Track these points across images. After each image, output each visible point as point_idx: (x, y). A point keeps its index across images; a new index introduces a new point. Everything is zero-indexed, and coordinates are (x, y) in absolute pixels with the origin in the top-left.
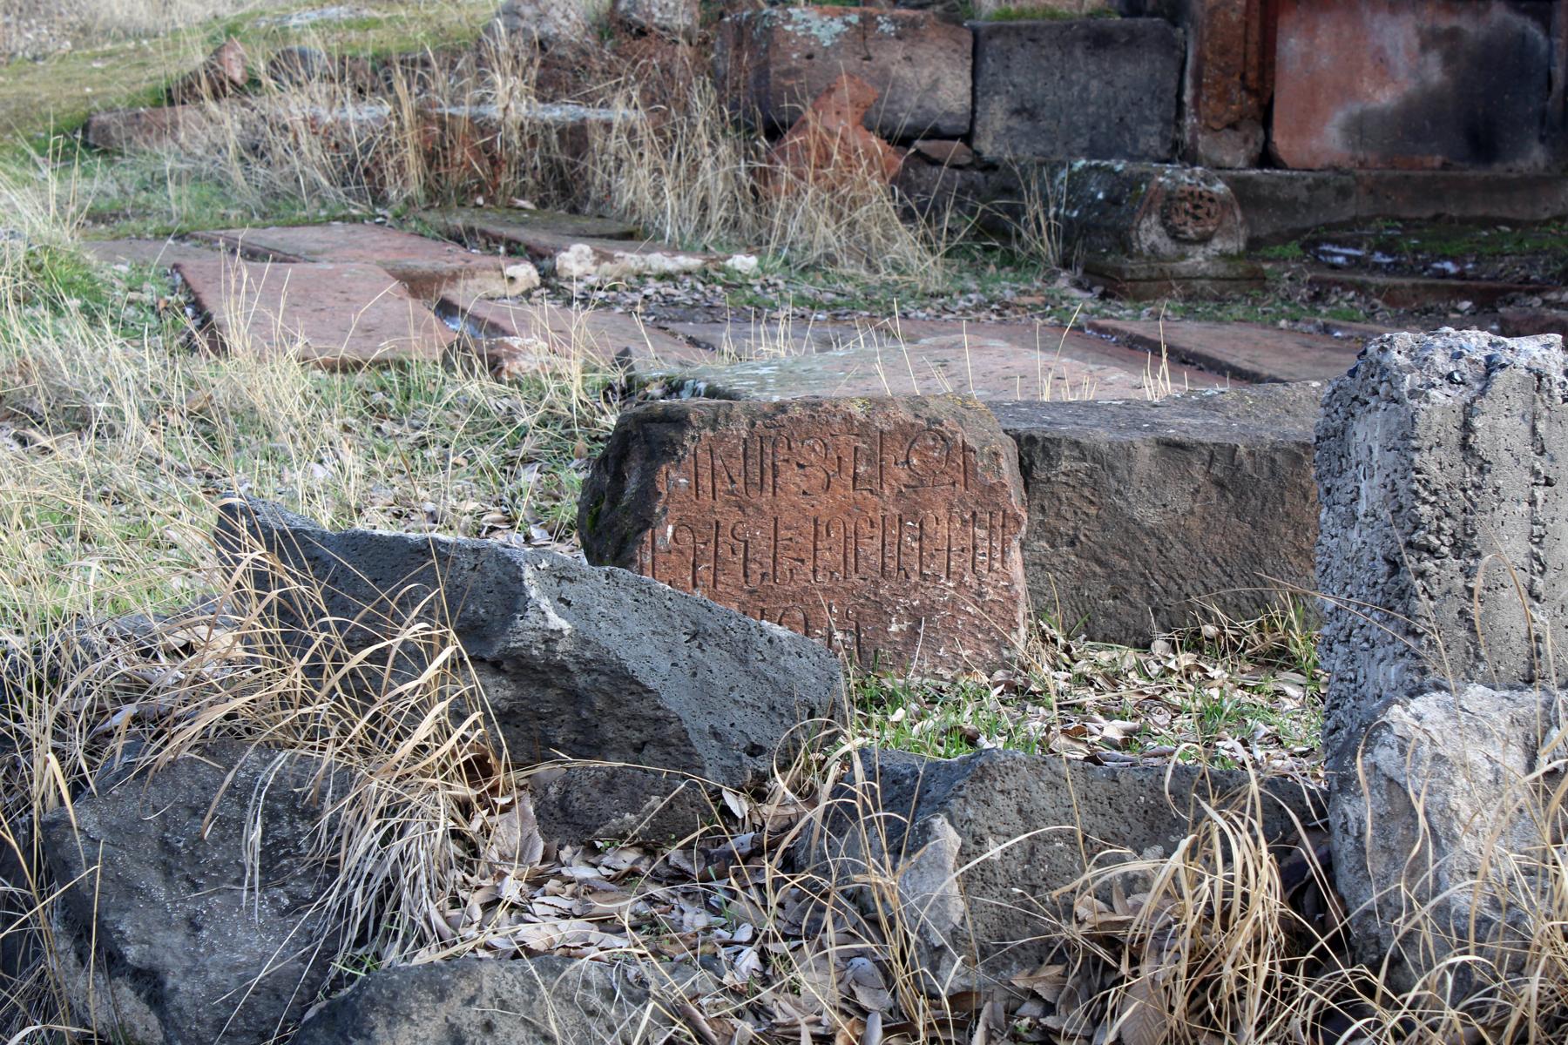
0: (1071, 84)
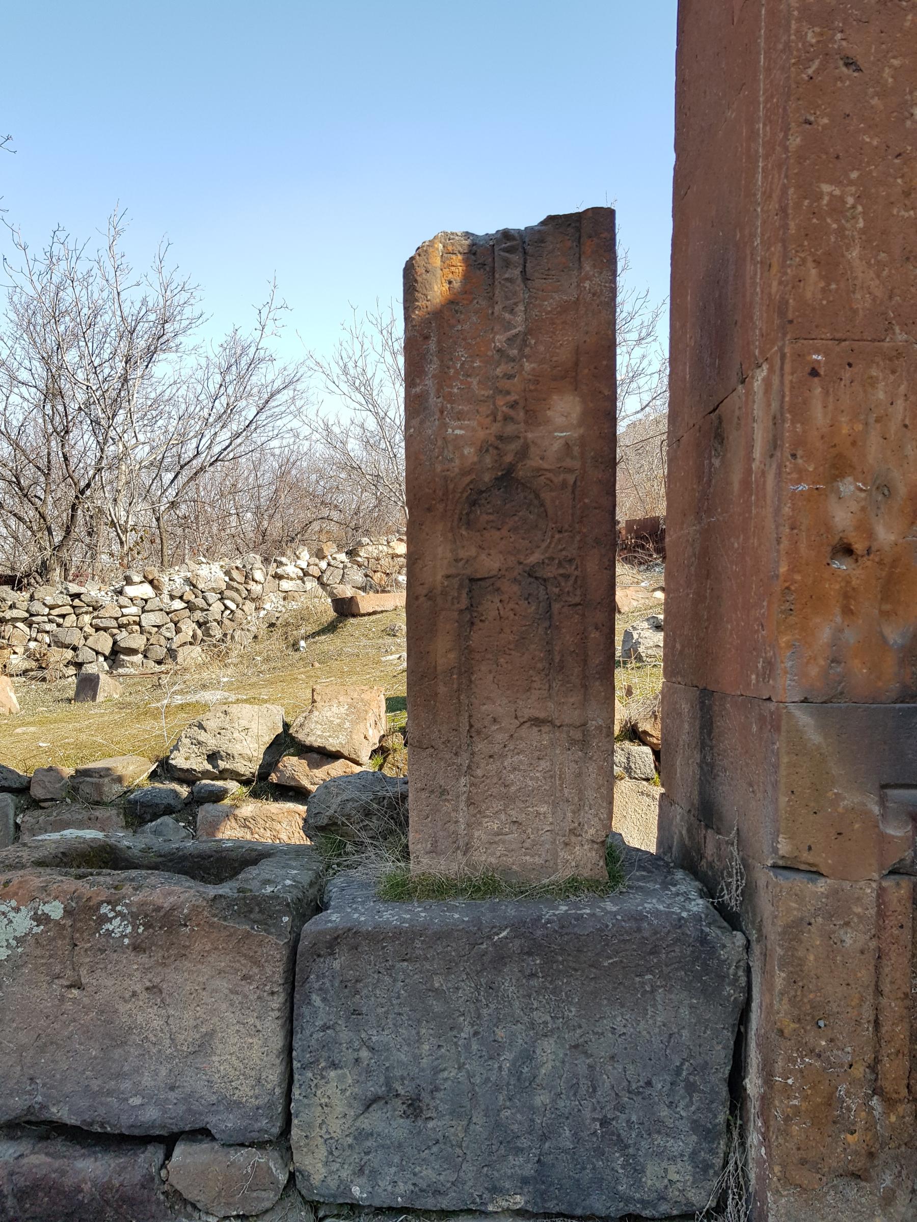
0: (494, 1050)
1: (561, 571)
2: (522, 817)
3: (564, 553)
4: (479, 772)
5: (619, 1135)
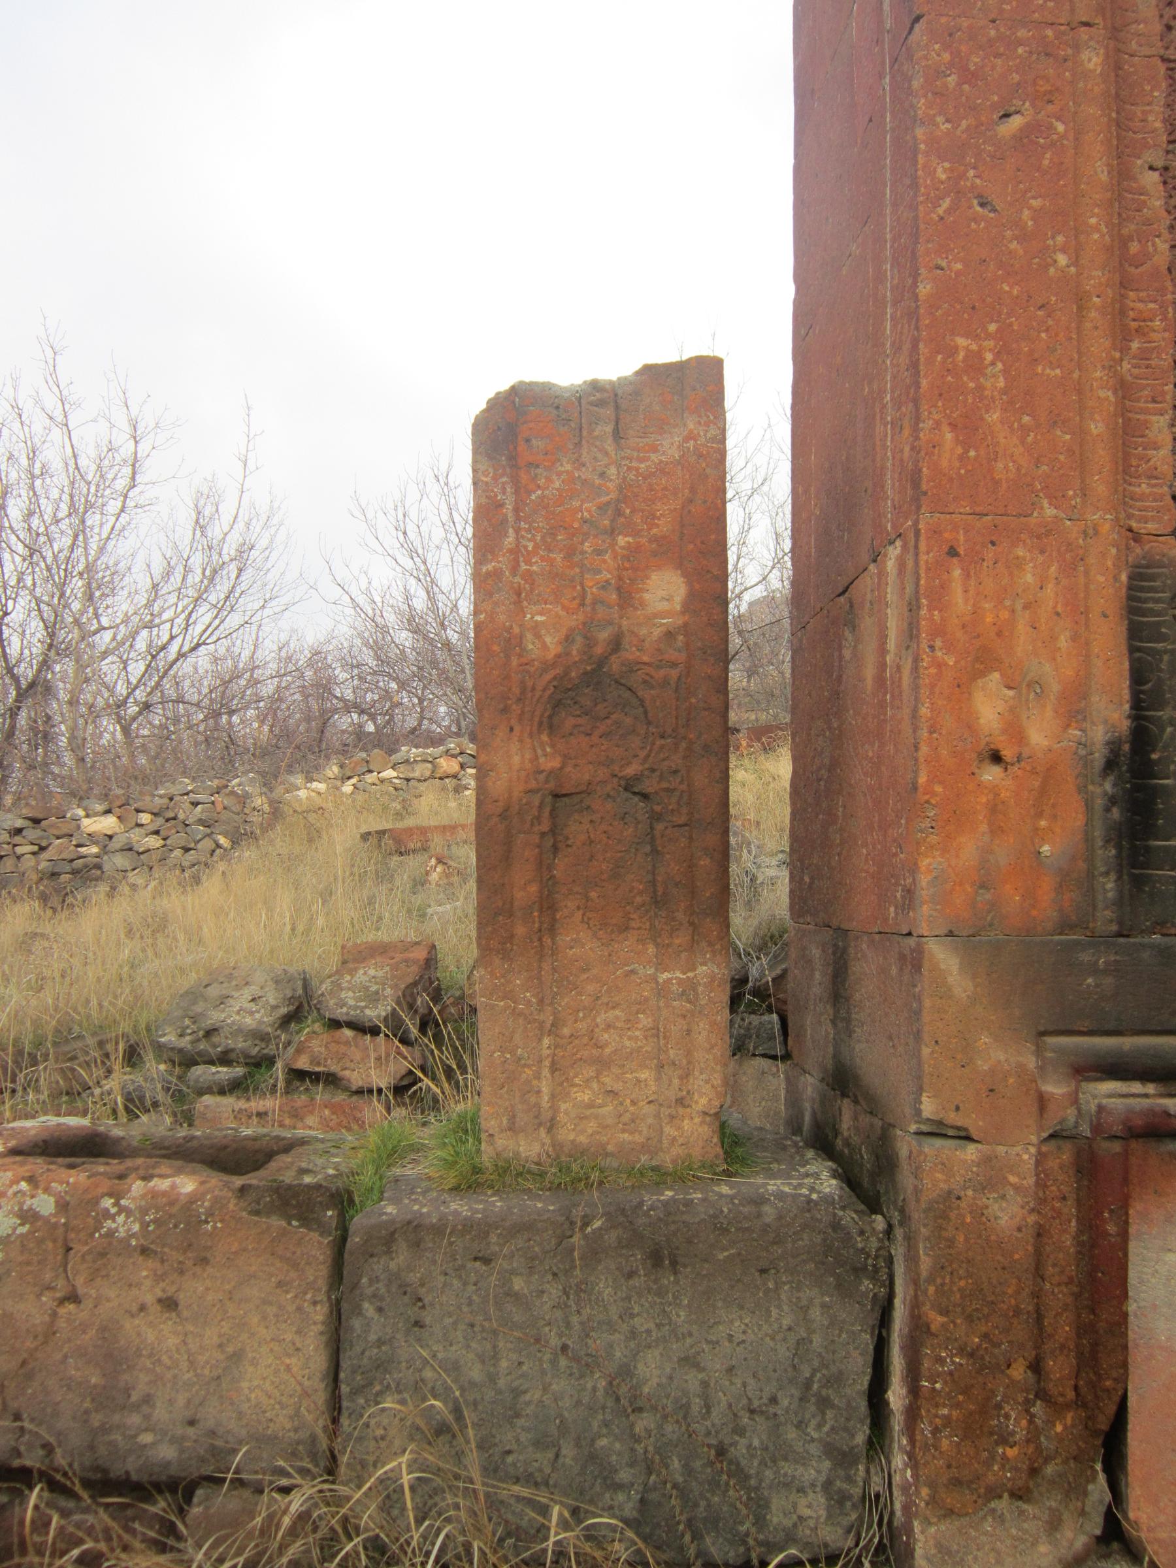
1: (665, 785)
2: (618, 1086)
3: (666, 763)
4: (566, 1031)
5: (738, 1464)
